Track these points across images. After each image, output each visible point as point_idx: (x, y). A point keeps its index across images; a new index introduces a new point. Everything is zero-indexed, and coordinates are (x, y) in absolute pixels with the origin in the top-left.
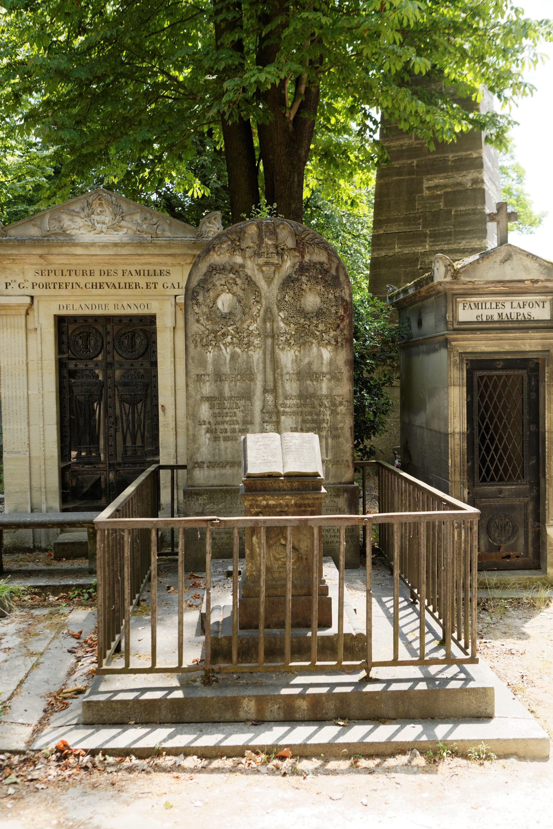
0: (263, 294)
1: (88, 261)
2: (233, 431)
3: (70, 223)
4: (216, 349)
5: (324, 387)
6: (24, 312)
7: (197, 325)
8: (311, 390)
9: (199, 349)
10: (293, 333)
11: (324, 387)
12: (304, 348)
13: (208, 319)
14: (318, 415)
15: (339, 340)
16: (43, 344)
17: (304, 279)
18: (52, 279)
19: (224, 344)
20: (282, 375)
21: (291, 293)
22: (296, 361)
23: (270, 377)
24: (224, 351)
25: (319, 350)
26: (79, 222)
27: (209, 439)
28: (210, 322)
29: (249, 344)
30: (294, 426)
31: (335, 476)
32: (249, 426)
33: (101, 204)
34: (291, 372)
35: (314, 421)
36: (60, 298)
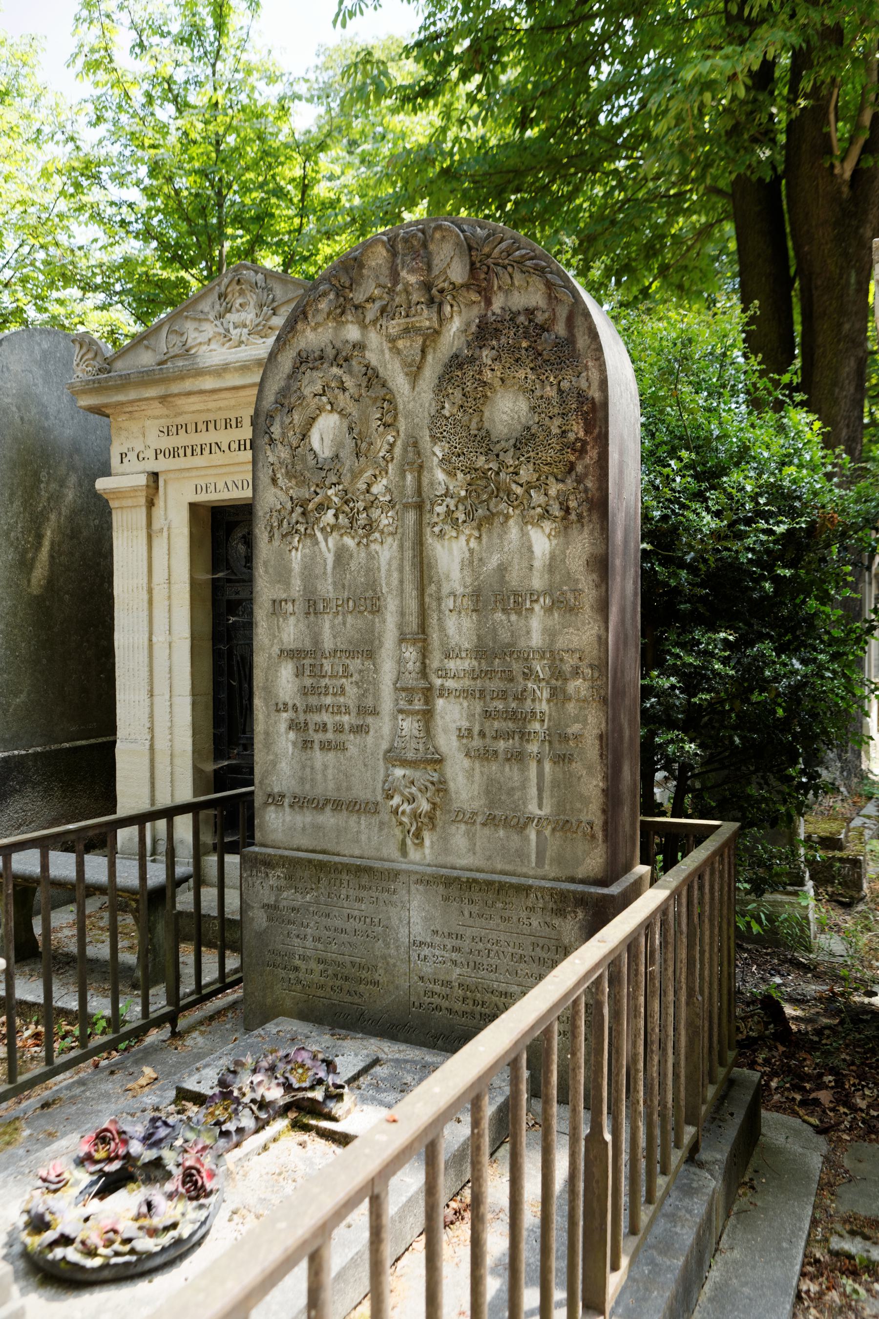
0: (401, 407)
1: (233, 402)
2: (339, 729)
3: (196, 334)
4: (308, 542)
5: (536, 628)
6: (143, 501)
7: (273, 490)
8: (504, 636)
9: (276, 543)
10: (463, 493)
11: (536, 628)
12: (490, 530)
13: (289, 475)
14: (520, 698)
15: (573, 504)
16: (173, 555)
17: (486, 355)
18: (182, 440)
19: (322, 530)
20: (439, 599)
21: (458, 393)
22: (471, 562)
23: (412, 605)
24: (323, 544)
25: (524, 534)
26: (209, 329)
27: (294, 744)
28: (294, 482)
29: (370, 527)
30: (465, 724)
31: (559, 860)
32: (370, 720)
33: (242, 292)
34: (460, 590)
35: (512, 716)
36: (194, 473)
